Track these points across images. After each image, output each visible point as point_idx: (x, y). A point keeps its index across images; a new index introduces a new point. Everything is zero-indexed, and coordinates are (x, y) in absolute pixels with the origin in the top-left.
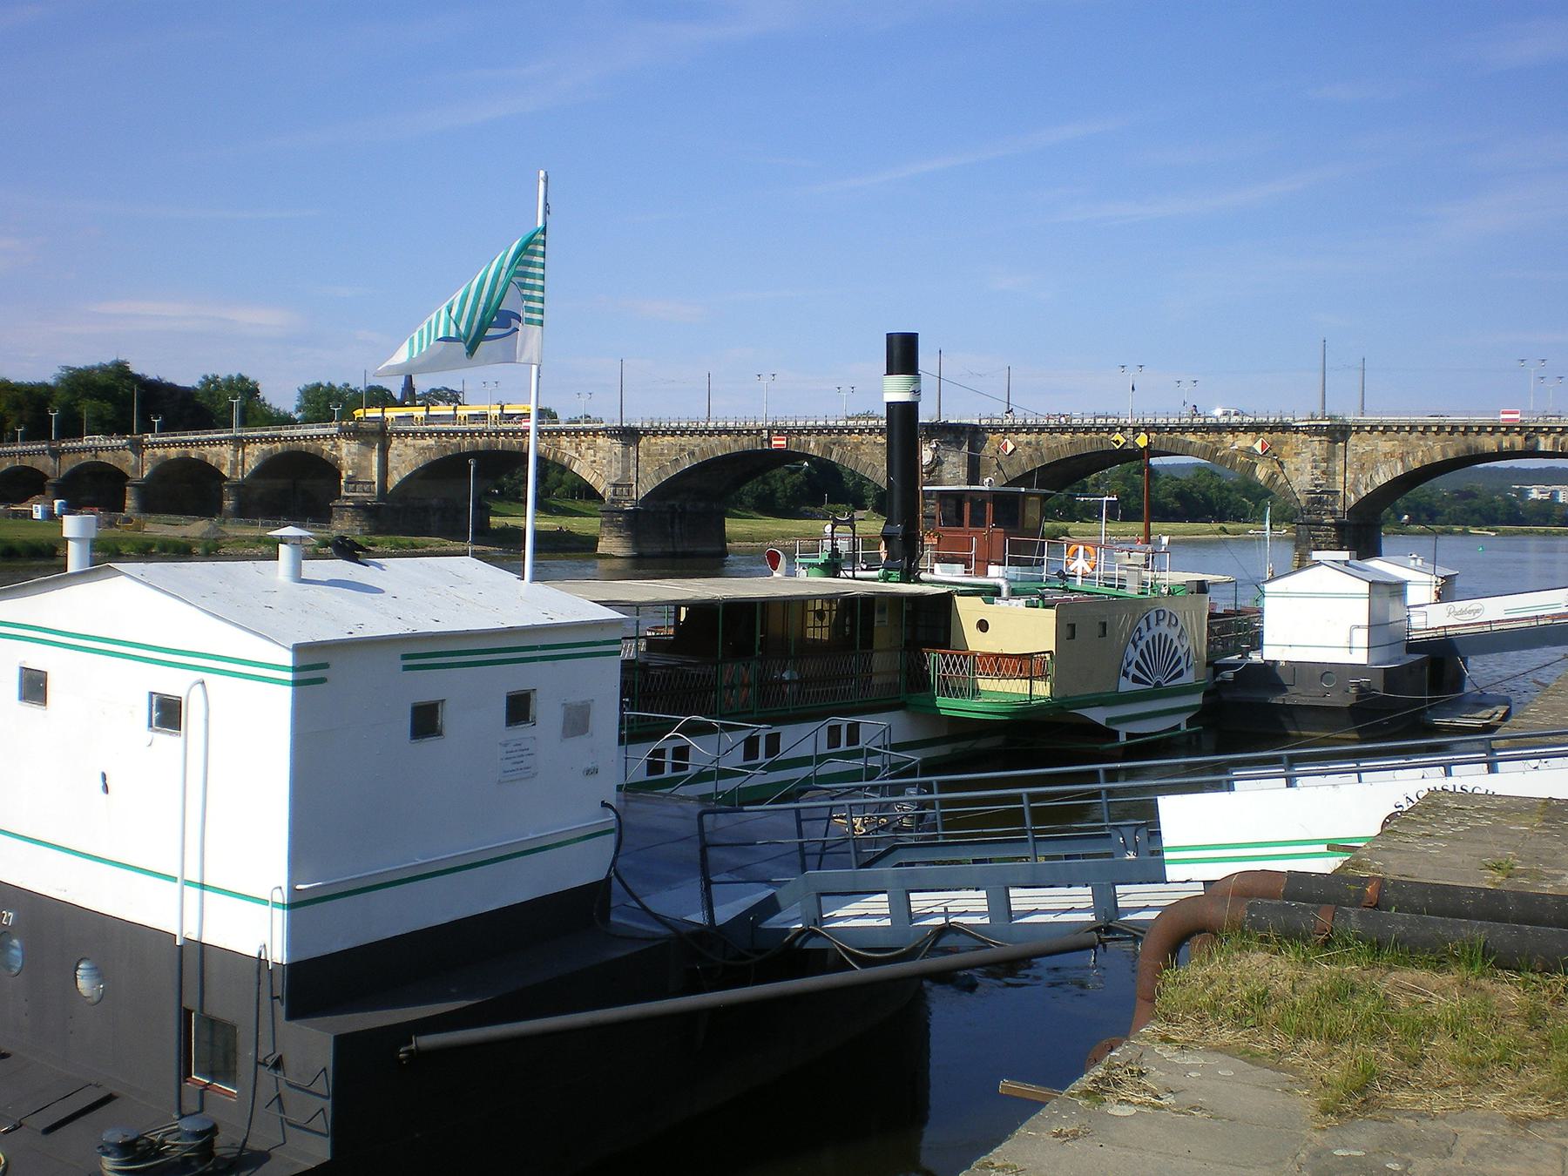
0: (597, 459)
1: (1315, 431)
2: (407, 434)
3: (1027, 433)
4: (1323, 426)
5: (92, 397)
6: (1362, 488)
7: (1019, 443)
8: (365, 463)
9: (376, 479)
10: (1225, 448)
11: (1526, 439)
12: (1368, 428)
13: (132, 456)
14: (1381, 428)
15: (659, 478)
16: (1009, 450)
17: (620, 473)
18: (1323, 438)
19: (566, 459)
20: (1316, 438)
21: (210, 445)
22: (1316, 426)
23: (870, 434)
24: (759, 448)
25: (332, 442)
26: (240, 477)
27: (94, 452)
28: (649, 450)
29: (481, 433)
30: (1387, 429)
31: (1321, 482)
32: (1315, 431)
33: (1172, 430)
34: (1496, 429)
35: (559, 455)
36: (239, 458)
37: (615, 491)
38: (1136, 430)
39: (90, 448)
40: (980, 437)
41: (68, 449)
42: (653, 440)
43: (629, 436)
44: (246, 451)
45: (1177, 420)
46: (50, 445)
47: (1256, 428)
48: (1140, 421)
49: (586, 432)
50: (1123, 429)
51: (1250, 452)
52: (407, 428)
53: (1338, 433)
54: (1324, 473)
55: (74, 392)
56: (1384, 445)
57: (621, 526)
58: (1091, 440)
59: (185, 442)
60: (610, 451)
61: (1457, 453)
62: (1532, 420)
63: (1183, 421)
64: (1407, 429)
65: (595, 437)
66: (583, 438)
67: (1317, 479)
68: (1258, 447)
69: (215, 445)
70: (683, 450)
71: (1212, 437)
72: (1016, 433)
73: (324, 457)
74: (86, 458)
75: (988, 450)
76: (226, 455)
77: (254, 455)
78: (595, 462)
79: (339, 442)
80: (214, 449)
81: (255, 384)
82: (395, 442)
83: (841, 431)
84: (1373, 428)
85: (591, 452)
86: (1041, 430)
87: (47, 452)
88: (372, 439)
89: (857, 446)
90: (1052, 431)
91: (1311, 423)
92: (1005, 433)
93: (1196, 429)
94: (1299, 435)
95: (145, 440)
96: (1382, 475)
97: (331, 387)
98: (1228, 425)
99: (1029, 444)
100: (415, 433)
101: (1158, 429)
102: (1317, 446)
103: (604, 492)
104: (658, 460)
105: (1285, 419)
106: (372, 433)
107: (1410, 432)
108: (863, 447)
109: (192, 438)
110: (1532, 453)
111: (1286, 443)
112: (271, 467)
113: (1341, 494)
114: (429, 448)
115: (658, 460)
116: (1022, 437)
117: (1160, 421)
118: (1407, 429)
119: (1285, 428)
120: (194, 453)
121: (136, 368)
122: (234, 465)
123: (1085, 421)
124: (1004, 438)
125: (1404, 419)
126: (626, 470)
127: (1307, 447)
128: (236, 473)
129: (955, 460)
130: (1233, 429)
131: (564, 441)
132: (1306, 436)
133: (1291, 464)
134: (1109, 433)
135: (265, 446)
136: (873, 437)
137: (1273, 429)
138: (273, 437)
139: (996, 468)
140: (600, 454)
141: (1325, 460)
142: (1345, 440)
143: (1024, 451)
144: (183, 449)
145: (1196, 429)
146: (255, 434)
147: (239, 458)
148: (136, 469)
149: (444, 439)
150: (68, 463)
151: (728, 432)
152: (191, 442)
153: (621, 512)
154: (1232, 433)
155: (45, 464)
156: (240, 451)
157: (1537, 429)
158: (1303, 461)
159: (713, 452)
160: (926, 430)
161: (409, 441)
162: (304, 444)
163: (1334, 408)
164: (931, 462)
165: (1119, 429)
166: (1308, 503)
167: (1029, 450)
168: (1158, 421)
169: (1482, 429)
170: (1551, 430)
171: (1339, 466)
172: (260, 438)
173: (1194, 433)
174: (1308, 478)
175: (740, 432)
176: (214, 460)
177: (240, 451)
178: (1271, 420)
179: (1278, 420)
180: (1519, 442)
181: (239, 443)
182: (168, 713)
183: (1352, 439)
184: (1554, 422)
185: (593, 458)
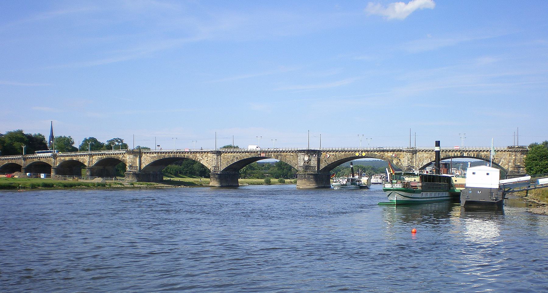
0: (208, 160)
1: (409, 152)
2: (148, 153)
5: (18, 141)
6: (420, 166)
7: (331, 155)
8: (135, 161)
9: (138, 166)
10: (385, 156)
11: (461, 153)
12: (422, 151)
13: (53, 160)
15: (227, 165)
16: (328, 157)
17: (216, 163)
18: (410, 153)
19: (199, 160)
20: (408, 153)
21: (80, 156)
23: (289, 152)
24: (257, 156)
25: (122, 155)
26: (91, 166)
27: (39, 158)
28: (224, 157)
29: (172, 153)
30: (427, 151)
31: (410, 164)
32: (409, 152)
34: (453, 151)
35: (196, 159)
36: (91, 160)
37: (215, 168)
39: (37, 157)
40: (320, 153)
41: (29, 158)
42: (225, 154)
43: (218, 153)
44: (93, 158)
45: (376, 149)
46: (23, 156)
47: (393, 151)
48: (363, 149)
49: (205, 152)
50: (359, 151)
51: (391, 157)
52: (147, 151)
53: (414, 152)
54: (411, 162)
55: (11, 140)
56: (426, 155)
57: (217, 178)
59: (72, 155)
60: (212, 157)
62: (461, 149)
64: (431, 151)
65: (207, 153)
66: (204, 154)
67: (409, 163)
68: (394, 155)
69: (82, 156)
70: (234, 157)
71: (382, 153)
72: (330, 152)
73: (120, 160)
74: (36, 160)
75: (322, 157)
76: (86, 159)
77: (95, 159)
78: (207, 160)
79: (125, 155)
80: (82, 157)
81: (43, 136)
82: (144, 155)
83: (281, 152)
84: (423, 151)
85: (206, 158)
86: (337, 151)
87: (22, 158)
88: (137, 154)
89: (285, 156)
90: (340, 152)
91: (408, 150)
93: (378, 151)
94: (404, 153)
95: (57, 155)
97: (65, 137)
98: (386, 150)
100: (150, 153)
101: (368, 151)
102: (409, 155)
103: (211, 169)
104: (227, 160)
105: (400, 149)
106: (137, 152)
108: (287, 156)
109: (74, 154)
110: (462, 157)
111: (401, 155)
112: (101, 163)
113: (415, 167)
114: (155, 157)
115: (227, 160)
116: (331, 153)
117: (369, 149)
118: (431, 151)
119: (401, 151)
120: (75, 159)
121: (25, 133)
122: (89, 162)
123: (349, 149)
125: (427, 149)
126: (217, 163)
128: (90, 164)
129: (314, 159)
130: (387, 151)
131: (198, 155)
133: (402, 160)
134: (355, 152)
135: (99, 157)
136: (290, 153)
137: (398, 151)
138: (103, 154)
140: (209, 158)
141: (411, 159)
144: (71, 157)
145: (378, 151)
146: (96, 153)
147: (91, 160)
148: (54, 163)
149: (160, 154)
150: (29, 162)
151: (248, 152)
152: (74, 155)
153: (217, 174)
154: (387, 152)
155: (22, 163)
156: (91, 158)
157: (463, 151)
158: (405, 159)
159: (243, 158)
161: (148, 155)
162: (113, 156)
163: (413, 145)
166: (407, 169)
167: (333, 157)
168: (368, 149)
169: (450, 151)
171: (414, 160)
172: (98, 154)
173: (377, 152)
175: (252, 152)
176: (82, 161)
177: (91, 158)
178: (397, 149)
179: (399, 149)
180: (459, 154)
181: (91, 155)
182: (488, 174)
183: (418, 153)
185: (207, 160)
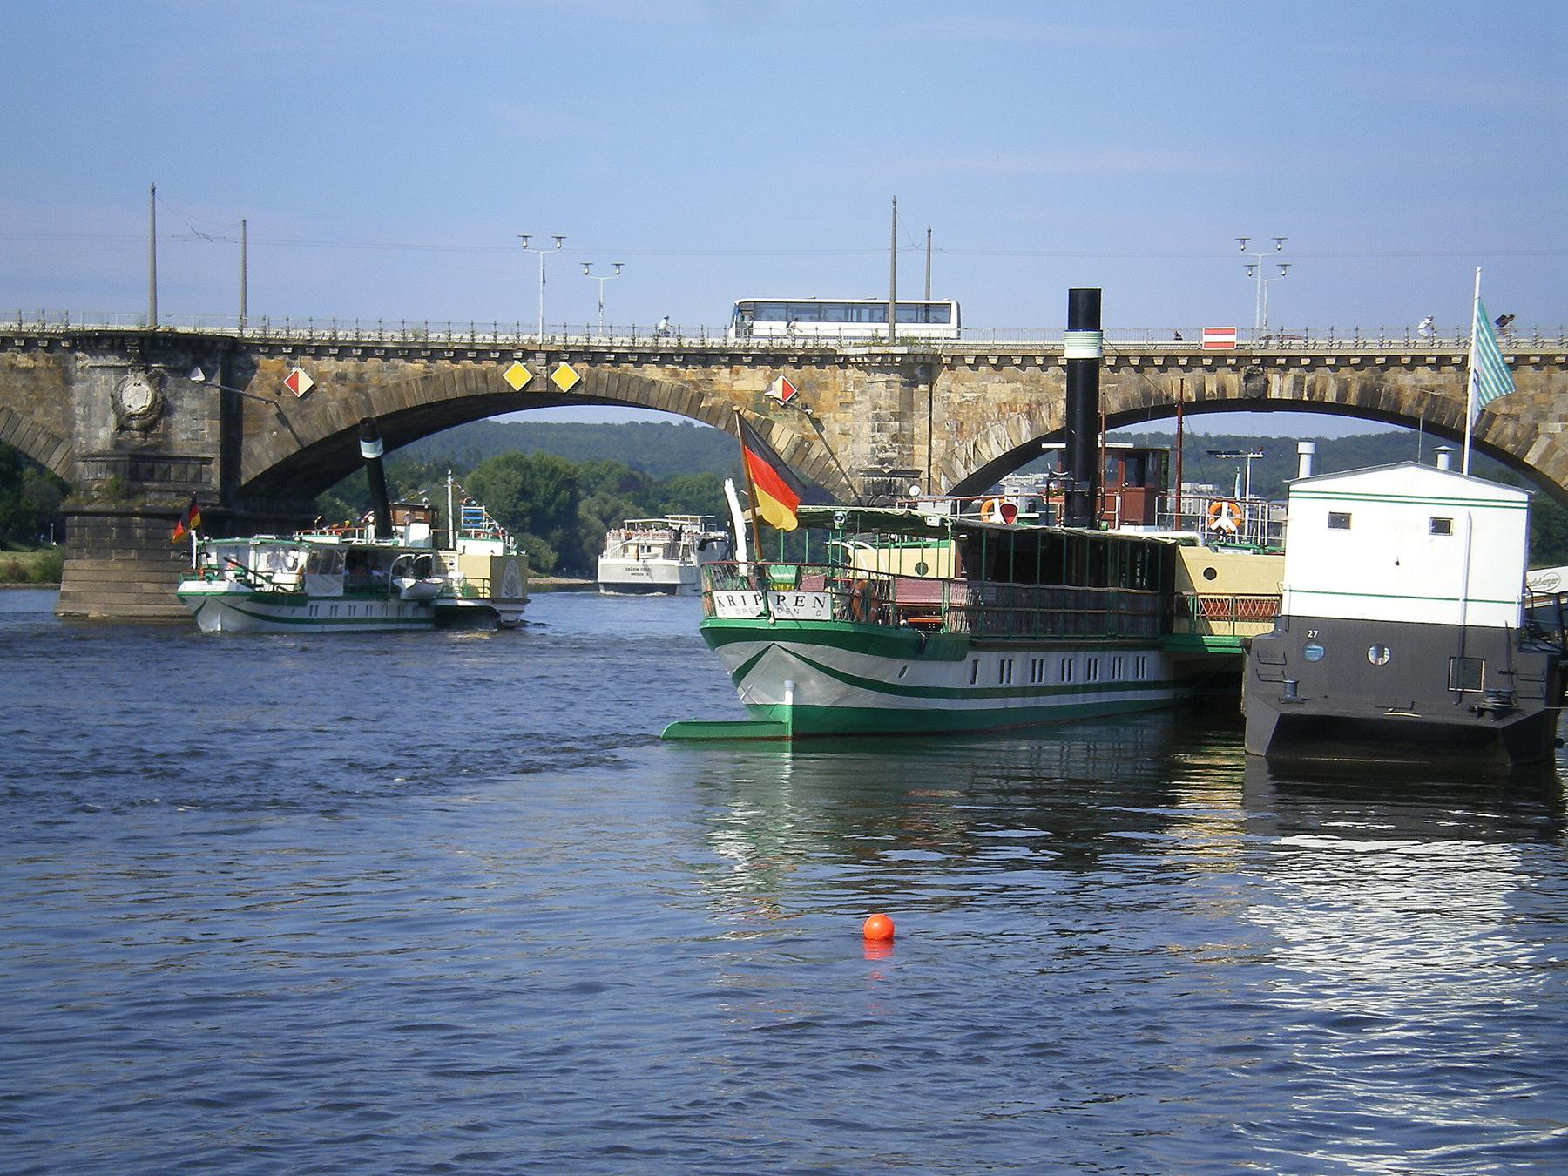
1: (884, 363)
3: (338, 357)
4: (893, 355)
10: (715, 394)
11: (1248, 377)
12: (970, 360)
14: (993, 360)
18: (893, 377)
20: (881, 377)
22: (883, 355)
30: (1004, 360)
31: (889, 455)
33: (620, 358)
34: (1194, 360)
38: (553, 357)
40: (241, 360)
45: (650, 341)
50: (528, 354)
51: (760, 401)
54: (895, 438)
56: (999, 390)
58: (466, 374)
61: (1126, 402)
62: (1253, 345)
63: (639, 342)
64: (1039, 361)
68: (777, 391)
71: (693, 373)
75: (259, 387)
84: (980, 359)
86: (368, 351)
90: (389, 353)
91: (875, 350)
92: (293, 355)
93: (664, 358)
96: (993, 442)
99: (341, 377)
101: (591, 356)
102: (883, 390)
107: (1043, 367)
110: (1259, 403)
111: (825, 385)
116: (328, 365)
117: (599, 341)
124: (290, 365)
127: (863, 393)
132: (862, 374)
133: (834, 423)
134: (499, 361)
139: (274, 423)
141: (899, 416)
142: (931, 382)
143: (333, 392)
157: (1268, 361)
158: (856, 417)
160: (141, 346)
164: (151, 409)
165: (520, 354)
167: (342, 391)
168: (594, 341)
169: (1170, 361)
170: (1292, 361)
171: (920, 426)
173: (660, 364)
174: (864, 448)
178: (799, 343)
180: (1234, 383)
183: (943, 380)
184: (1296, 348)
